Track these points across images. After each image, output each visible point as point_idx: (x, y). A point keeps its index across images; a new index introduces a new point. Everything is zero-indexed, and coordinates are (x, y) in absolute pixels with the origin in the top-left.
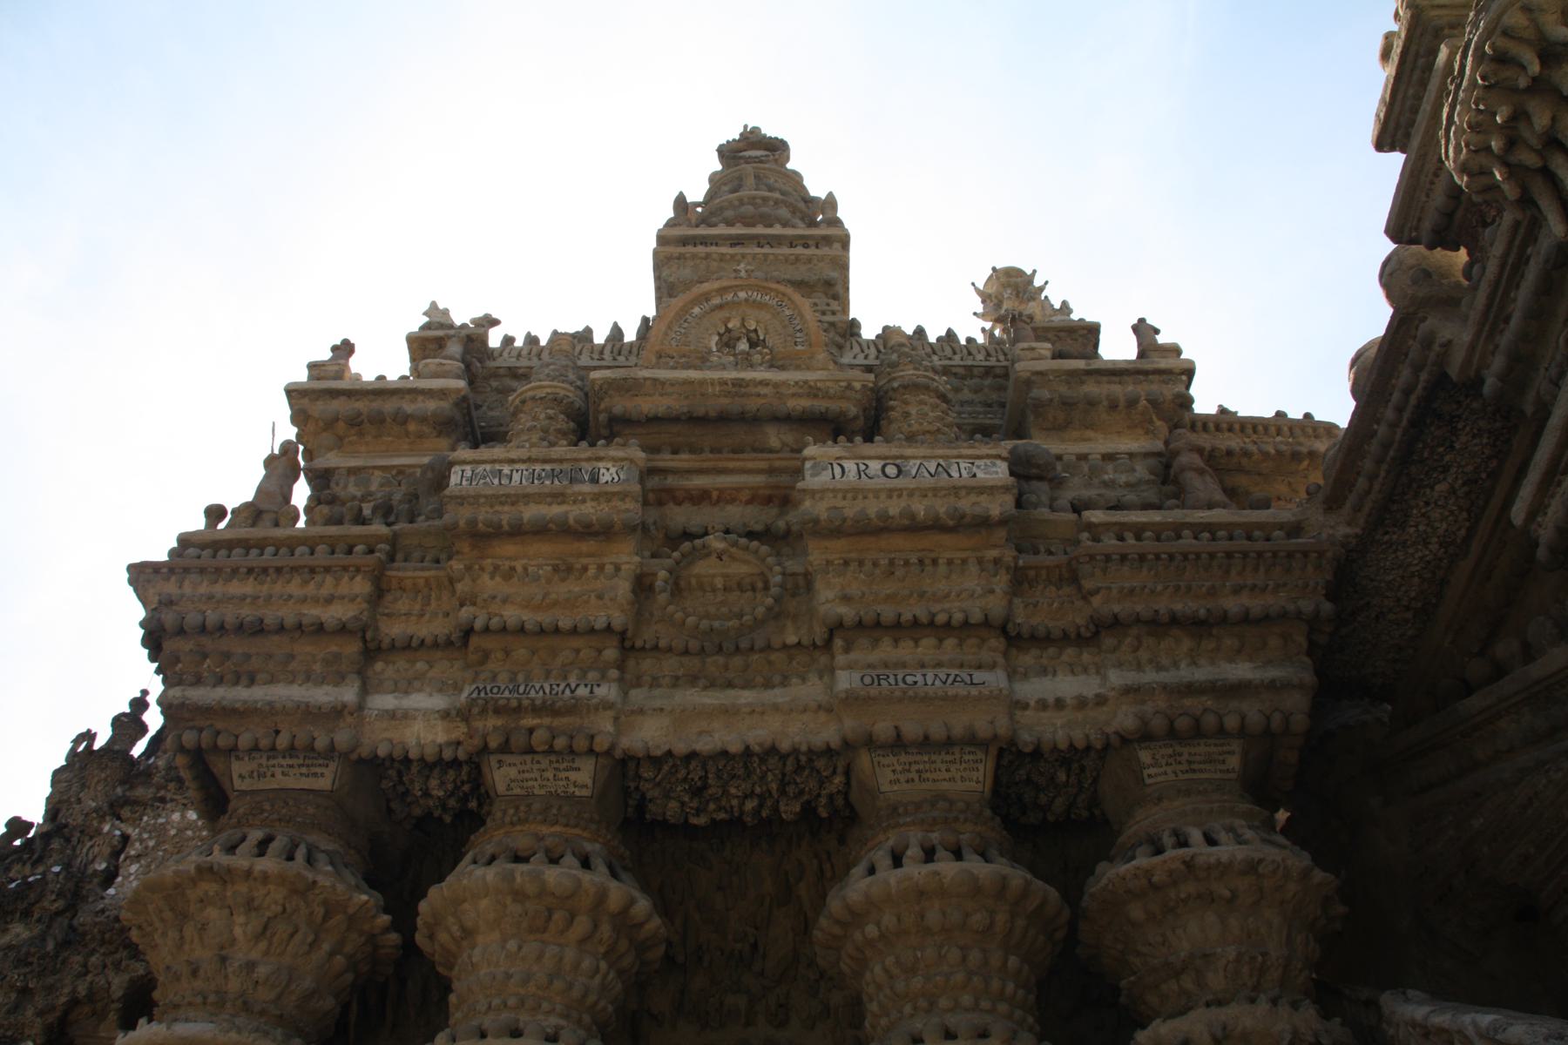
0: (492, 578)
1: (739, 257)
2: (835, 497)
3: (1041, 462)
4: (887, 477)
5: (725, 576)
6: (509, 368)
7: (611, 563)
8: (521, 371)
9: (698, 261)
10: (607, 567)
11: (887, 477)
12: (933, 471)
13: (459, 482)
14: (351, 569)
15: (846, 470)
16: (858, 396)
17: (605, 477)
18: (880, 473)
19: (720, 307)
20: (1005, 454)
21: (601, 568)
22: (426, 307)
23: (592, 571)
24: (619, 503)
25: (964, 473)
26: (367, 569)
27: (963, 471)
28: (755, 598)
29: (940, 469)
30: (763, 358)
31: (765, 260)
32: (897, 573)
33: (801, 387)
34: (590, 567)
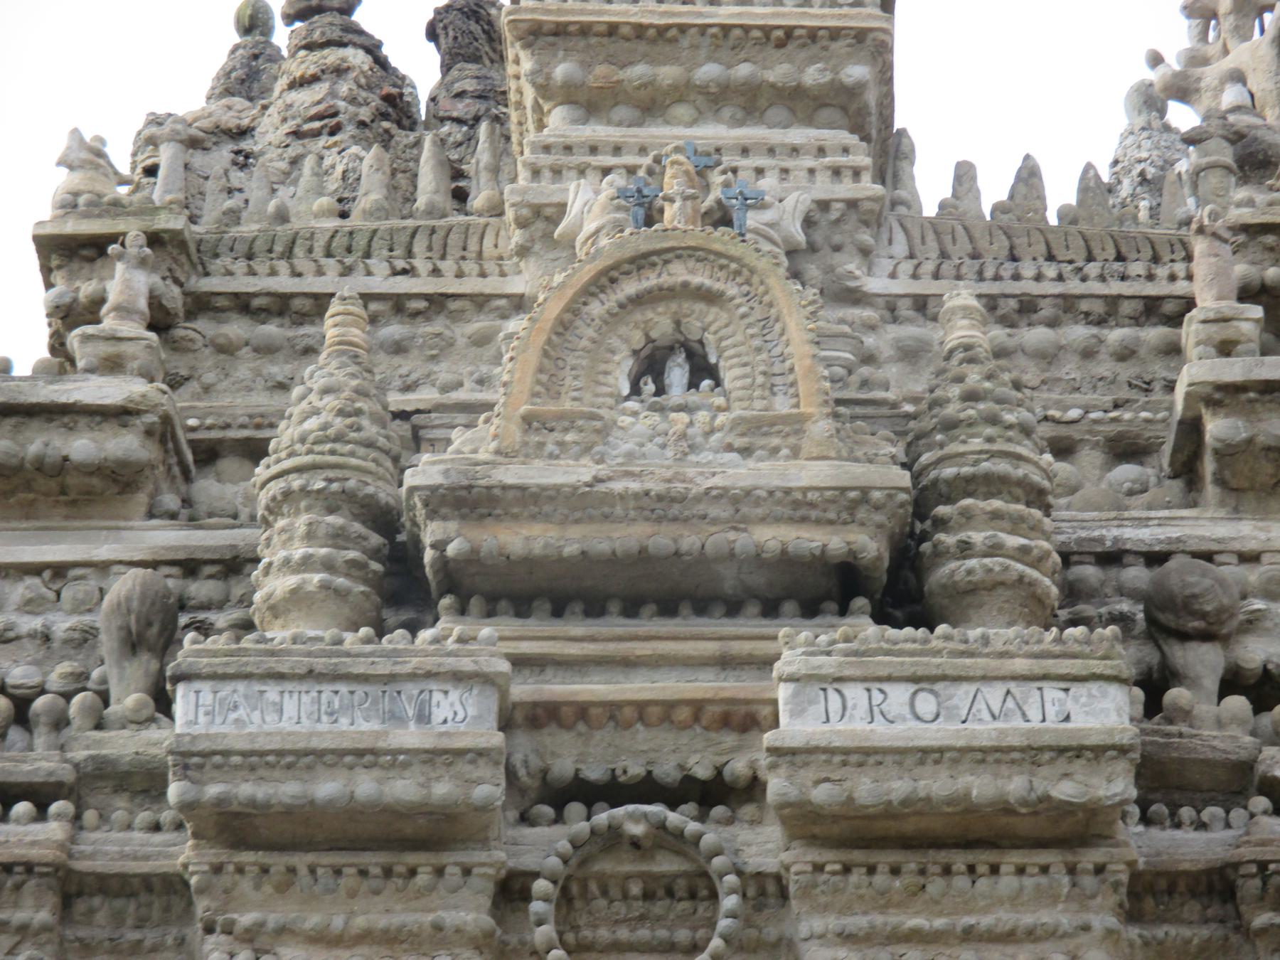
0: (257, 887)
1: (672, 33)
2: (828, 762)
3: (1208, 608)
4: (918, 718)
5: (642, 876)
6: (236, 295)
7: (456, 864)
8: (256, 302)
9: (593, 40)
10: (449, 870)
11: (918, 718)
12: (996, 709)
13: (191, 717)
14: (19, 869)
15: (850, 704)
16: (879, 518)
17: (439, 714)
18: (906, 711)
19: (638, 301)
20: (1129, 672)
21: (439, 872)
22: (60, 145)
23: (423, 878)
24: (469, 767)
25: (1051, 711)
26: (45, 870)
27: (1048, 706)
28: (695, 911)
29: (1010, 704)
30: (714, 418)
31: (726, 36)
32: (929, 888)
33: (779, 503)
34: (420, 870)
